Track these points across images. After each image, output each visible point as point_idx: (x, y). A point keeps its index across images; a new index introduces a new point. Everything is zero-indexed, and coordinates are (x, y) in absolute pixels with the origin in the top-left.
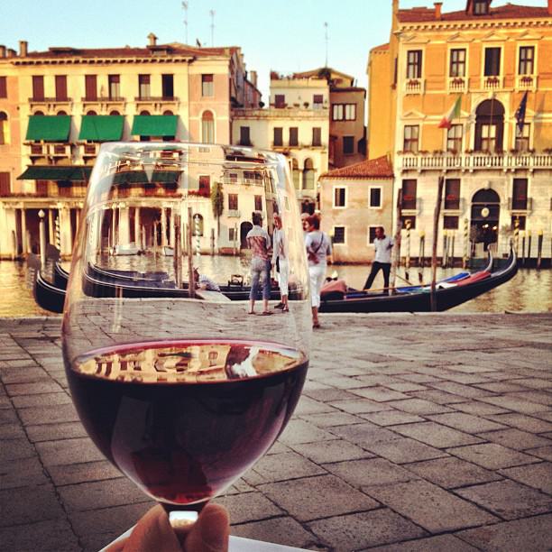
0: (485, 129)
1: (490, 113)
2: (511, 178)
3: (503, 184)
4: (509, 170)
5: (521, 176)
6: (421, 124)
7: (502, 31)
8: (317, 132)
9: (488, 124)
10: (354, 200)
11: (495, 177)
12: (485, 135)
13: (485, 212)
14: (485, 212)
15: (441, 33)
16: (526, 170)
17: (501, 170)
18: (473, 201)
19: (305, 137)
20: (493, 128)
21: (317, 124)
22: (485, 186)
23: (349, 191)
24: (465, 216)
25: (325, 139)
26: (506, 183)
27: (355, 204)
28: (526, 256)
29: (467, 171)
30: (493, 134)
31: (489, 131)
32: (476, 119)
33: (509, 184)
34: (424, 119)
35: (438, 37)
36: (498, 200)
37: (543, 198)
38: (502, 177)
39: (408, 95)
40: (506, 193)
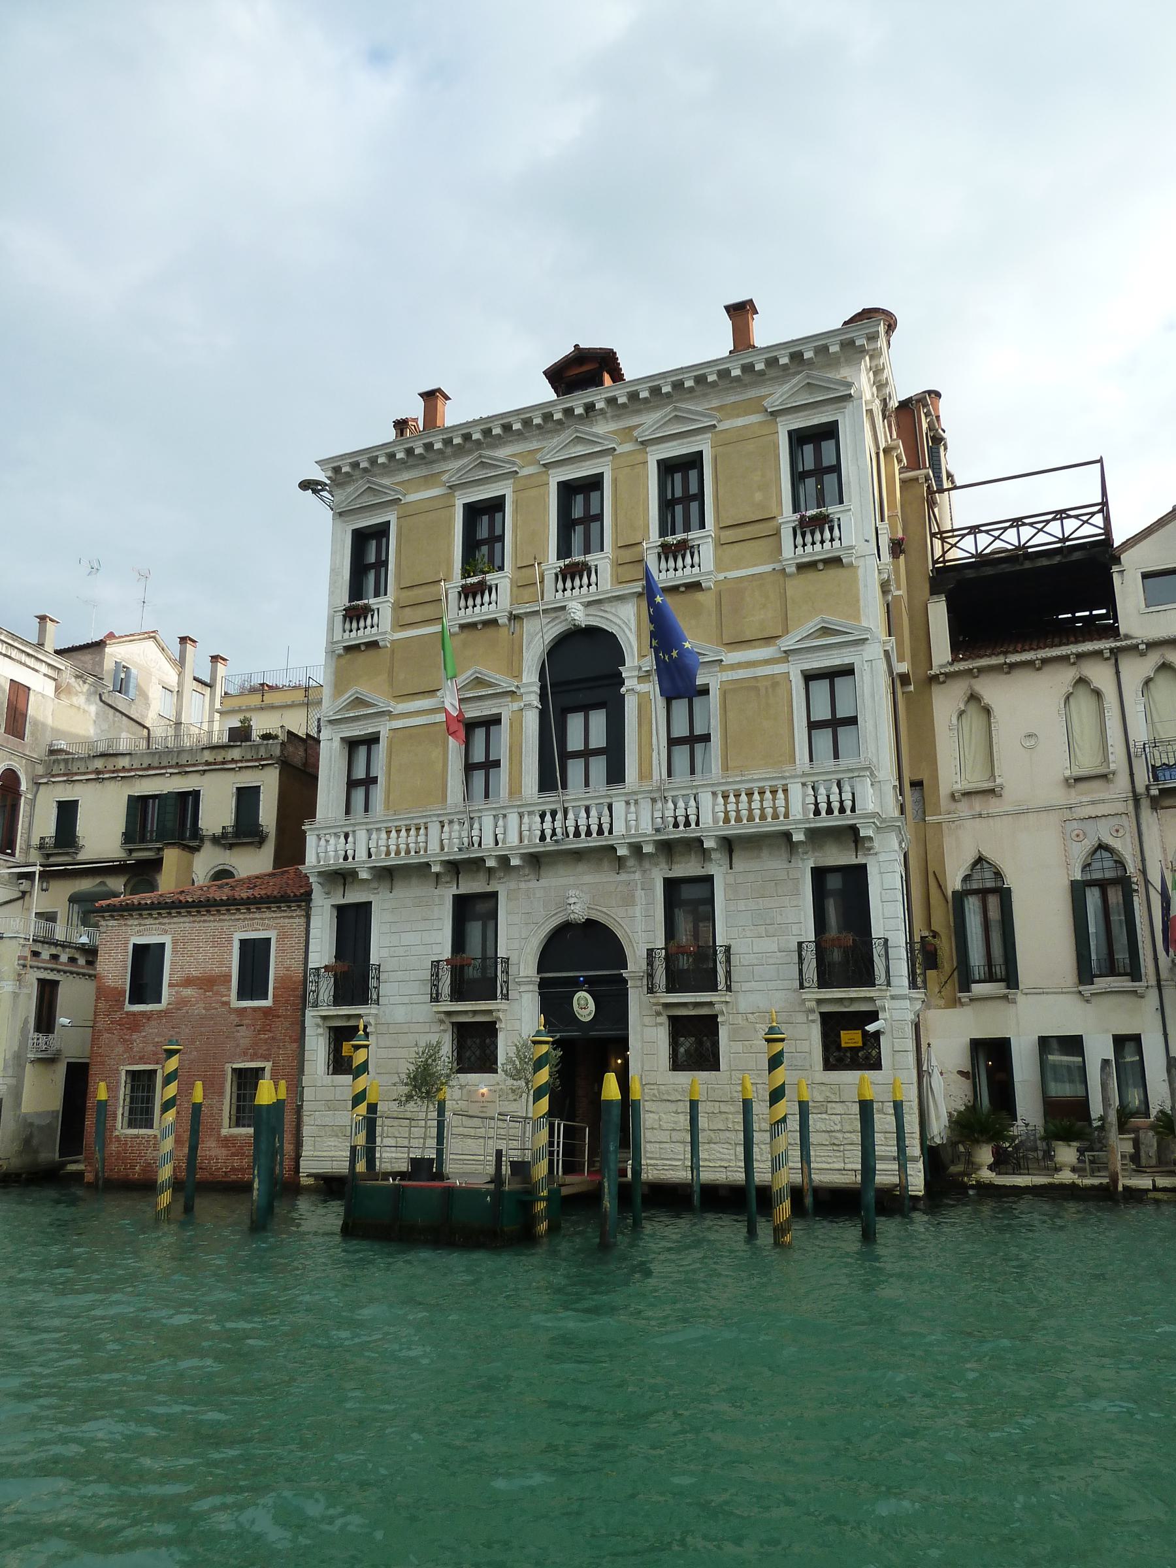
0: (575, 723)
1: (581, 672)
2: (658, 876)
3: (628, 901)
5: (687, 868)
6: (384, 728)
7: (602, 428)
8: (247, 798)
9: (586, 708)
10: (188, 982)
12: (575, 742)
13: (584, 1005)
15: (437, 468)
18: (540, 970)
19: (217, 813)
20: (598, 720)
21: (248, 779)
22: (579, 912)
23: (174, 951)
24: (520, 1019)
25: (268, 814)
26: (639, 893)
27: (188, 992)
28: (701, 1163)
30: (598, 739)
31: (585, 729)
33: (651, 903)
35: (429, 481)
37: (771, 945)
38: (623, 877)
39: (348, 649)
40: (641, 929)
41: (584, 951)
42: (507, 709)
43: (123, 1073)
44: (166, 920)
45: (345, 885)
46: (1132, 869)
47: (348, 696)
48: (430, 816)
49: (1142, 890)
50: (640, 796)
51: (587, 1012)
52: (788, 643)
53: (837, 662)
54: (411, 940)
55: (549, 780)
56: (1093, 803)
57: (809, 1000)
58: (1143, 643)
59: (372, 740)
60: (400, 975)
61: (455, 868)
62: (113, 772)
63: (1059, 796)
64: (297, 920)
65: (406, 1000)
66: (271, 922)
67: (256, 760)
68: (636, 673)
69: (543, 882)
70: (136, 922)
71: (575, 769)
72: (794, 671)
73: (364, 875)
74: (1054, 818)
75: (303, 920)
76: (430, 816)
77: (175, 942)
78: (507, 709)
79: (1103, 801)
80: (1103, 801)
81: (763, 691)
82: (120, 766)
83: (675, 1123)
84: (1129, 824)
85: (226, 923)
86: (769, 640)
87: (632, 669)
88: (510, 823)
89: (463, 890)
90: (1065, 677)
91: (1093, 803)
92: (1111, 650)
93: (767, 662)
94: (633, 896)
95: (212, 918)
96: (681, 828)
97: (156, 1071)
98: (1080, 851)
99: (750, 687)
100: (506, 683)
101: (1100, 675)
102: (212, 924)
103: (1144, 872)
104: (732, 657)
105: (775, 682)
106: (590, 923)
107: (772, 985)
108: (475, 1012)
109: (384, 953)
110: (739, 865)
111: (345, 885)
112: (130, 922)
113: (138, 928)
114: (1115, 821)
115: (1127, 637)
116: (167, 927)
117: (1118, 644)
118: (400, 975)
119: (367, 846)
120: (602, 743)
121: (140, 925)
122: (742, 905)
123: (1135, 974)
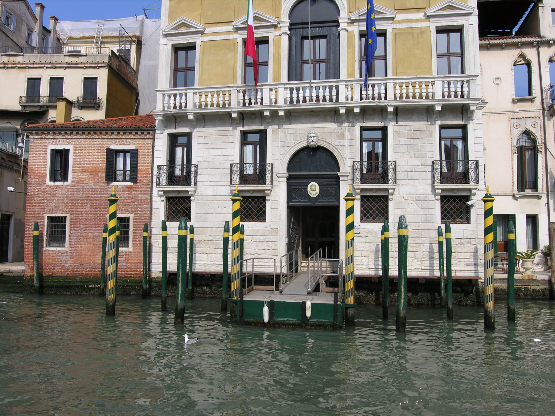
3: (342, 137)
4: (350, 111)
6: (198, 40)
8: (90, 84)
11: (330, 126)
12: (307, 55)
13: (314, 189)
14: (314, 189)
16: (381, 111)
17: (335, 111)
18: (288, 170)
19: (73, 89)
21: (91, 73)
23: (75, 153)
25: (102, 92)
26: (347, 134)
27: (85, 176)
29: (274, 113)
32: (290, 30)
34: (202, 33)
36: (337, 166)
37: (417, 162)
41: (314, 162)
42: (272, 35)
43: (46, 218)
44: (69, 137)
45: (176, 123)
46: (539, 141)
47: (177, 21)
48: (232, 87)
49: (544, 152)
50: (354, 83)
51: (314, 193)
52: (430, 12)
53: (455, 24)
54: (216, 154)
55: (295, 73)
56: (525, 111)
57: (438, 189)
58: (552, 40)
59: (192, 47)
60: (209, 171)
61: (243, 117)
62: (14, 64)
63: (510, 106)
64: (147, 140)
65: (213, 184)
66: (132, 141)
67: (95, 63)
68: (347, 20)
69: (293, 126)
70: (51, 137)
71: (308, 69)
72: (433, 25)
73: (191, 117)
74: (506, 117)
75: (151, 141)
76: (232, 87)
77: (75, 149)
78: (272, 35)
79: (529, 111)
80: (529, 111)
81: (416, 35)
82: (17, 61)
83: (364, 247)
84: (540, 122)
85: (105, 140)
86: (418, 9)
87: (344, 18)
88: (276, 93)
89: (246, 128)
90: (514, 53)
91: (525, 111)
92: (538, 42)
93: (418, 20)
94: (343, 135)
95: (97, 137)
96: (376, 100)
97: (65, 218)
98: (517, 132)
99: (410, 32)
100: (273, 21)
101: (530, 53)
102: (96, 140)
103: (545, 144)
104: (400, 17)
105: (423, 31)
106: (319, 148)
107: (417, 182)
108: (254, 191)
109: (200, 159)
110: (400, 123)
111: (176, 123)
112: (48, 137)
113: (52, 140)
114: (533, 120)
115: (544, 37)
116: (70, 140)
117: (539, 40)
118: (209, 171)
119: (192, 101)
120: (323, 56)
121: (54, 139)
122: (402, 142)
123: (535, 187)
